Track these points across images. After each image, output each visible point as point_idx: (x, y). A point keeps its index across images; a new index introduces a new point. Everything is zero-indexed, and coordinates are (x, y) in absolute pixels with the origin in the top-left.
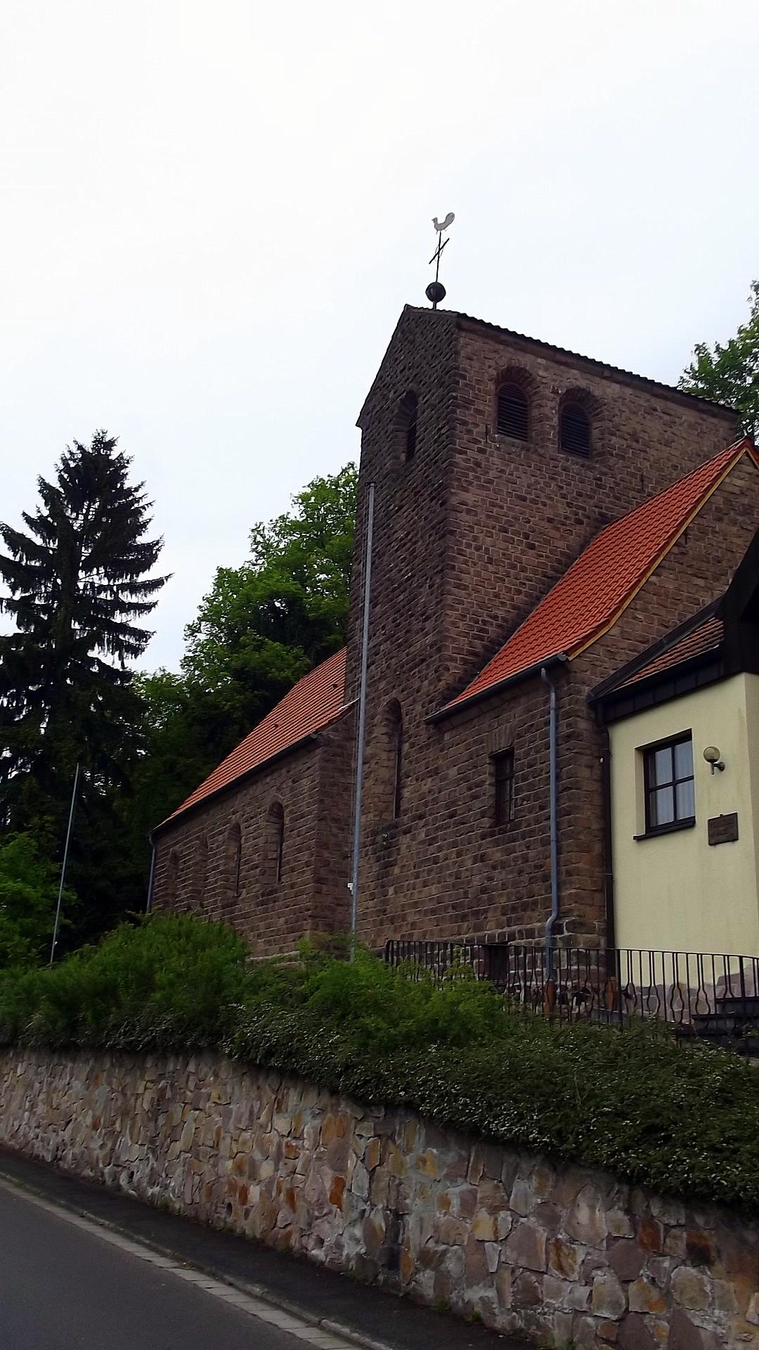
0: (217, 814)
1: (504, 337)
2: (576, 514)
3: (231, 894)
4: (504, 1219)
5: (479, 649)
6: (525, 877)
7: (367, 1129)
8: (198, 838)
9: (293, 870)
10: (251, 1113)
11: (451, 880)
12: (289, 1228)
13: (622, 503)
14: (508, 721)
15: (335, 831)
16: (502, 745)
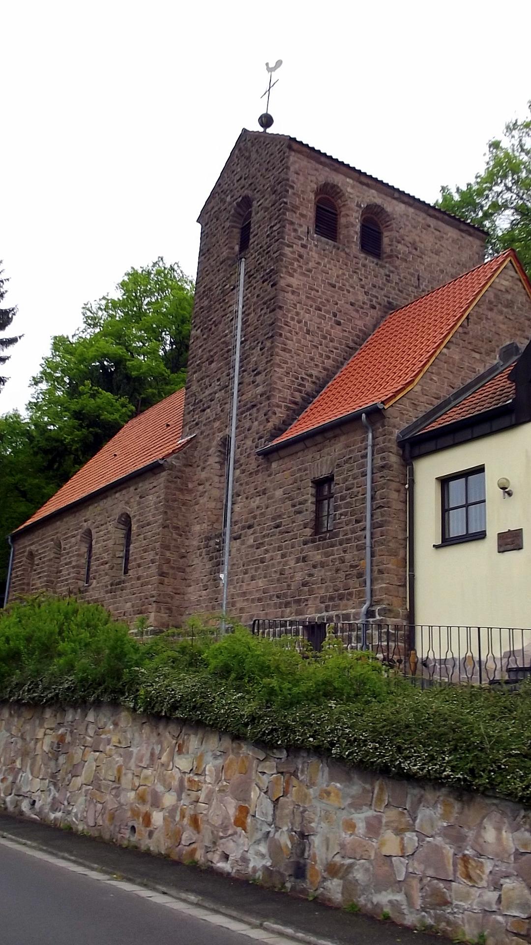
0: (70, 521)
1: (323, 159)
2: (371, 301)
3: (81, 583)
4: (411, 839)
5: (299, 399)
6: (342, 575)
7: (270, 767)
9: (139, 566)
10: (152, 754)
11: (276, 576)
12: (193, 846)
13: (404, 295)
14: (329, 454)
15: (175, 536)
16: (324, 472)
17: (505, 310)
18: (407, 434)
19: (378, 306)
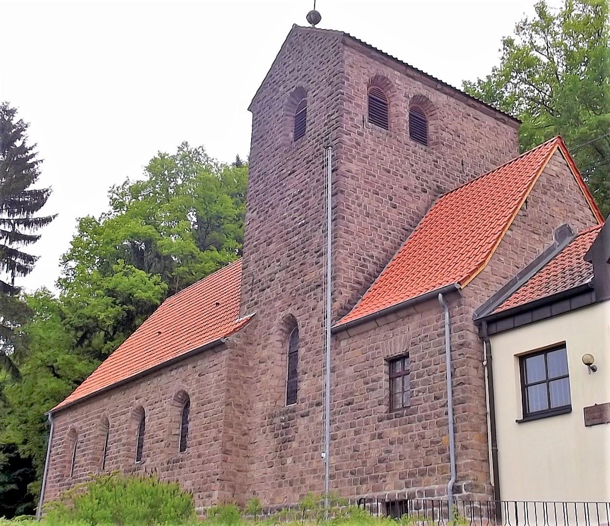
1: (373, 53)
5: (362, 280)
6: (422, 451)
8: (99, 417)
13: (451, 179)
15: (237, 413)
16: (399, 350)
17: (557, 193)
18: (482, 312)
19: (428, 190)
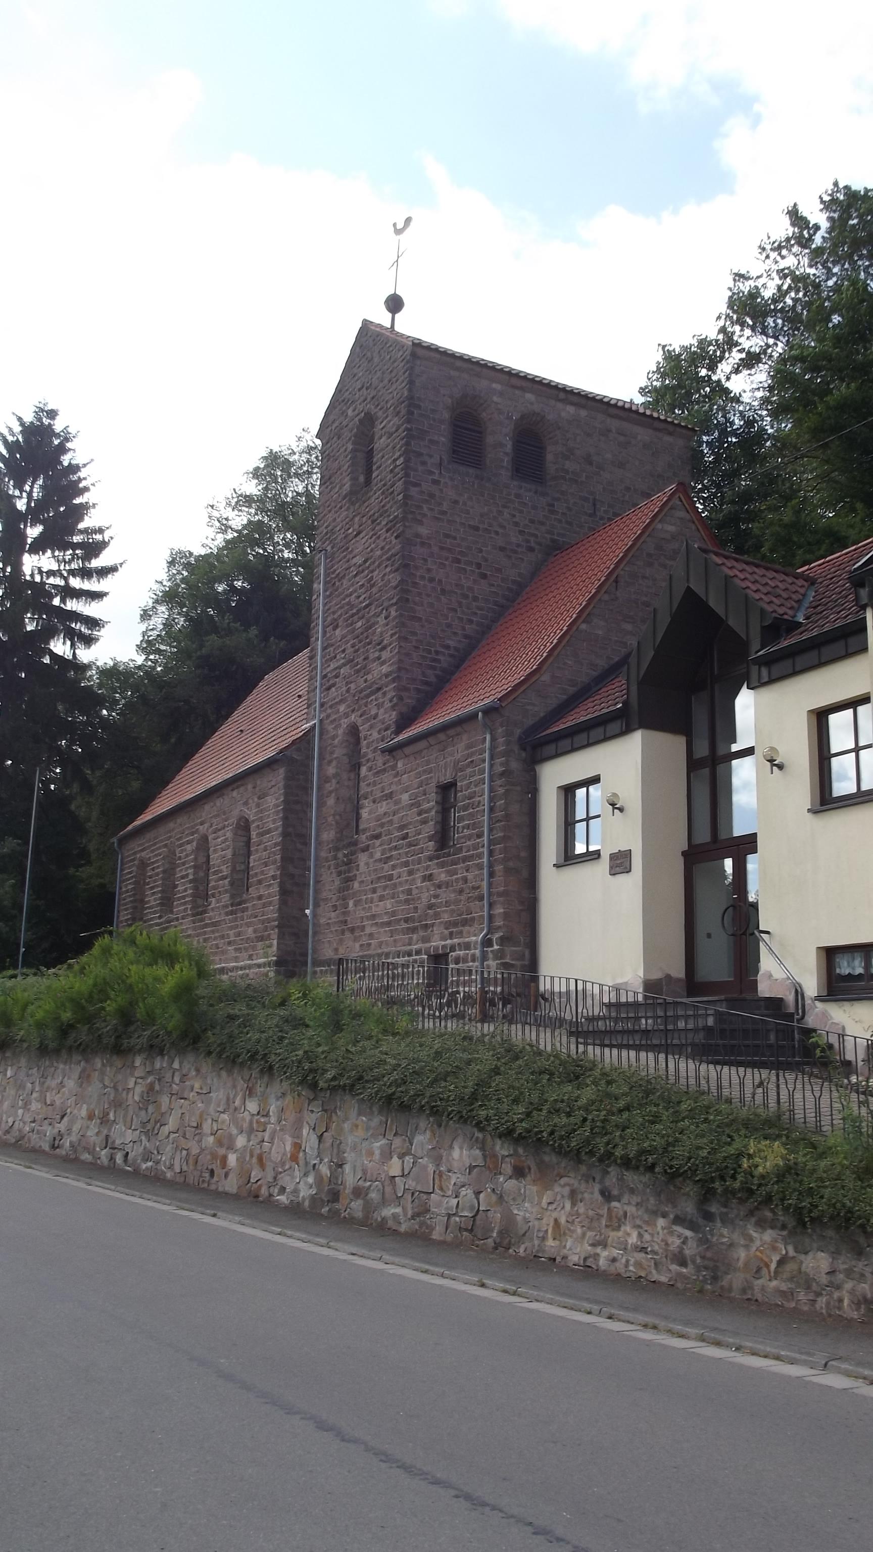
2: (528, 541)
5: (433, 679)
11: (403, 897)
14: (452, 755)
